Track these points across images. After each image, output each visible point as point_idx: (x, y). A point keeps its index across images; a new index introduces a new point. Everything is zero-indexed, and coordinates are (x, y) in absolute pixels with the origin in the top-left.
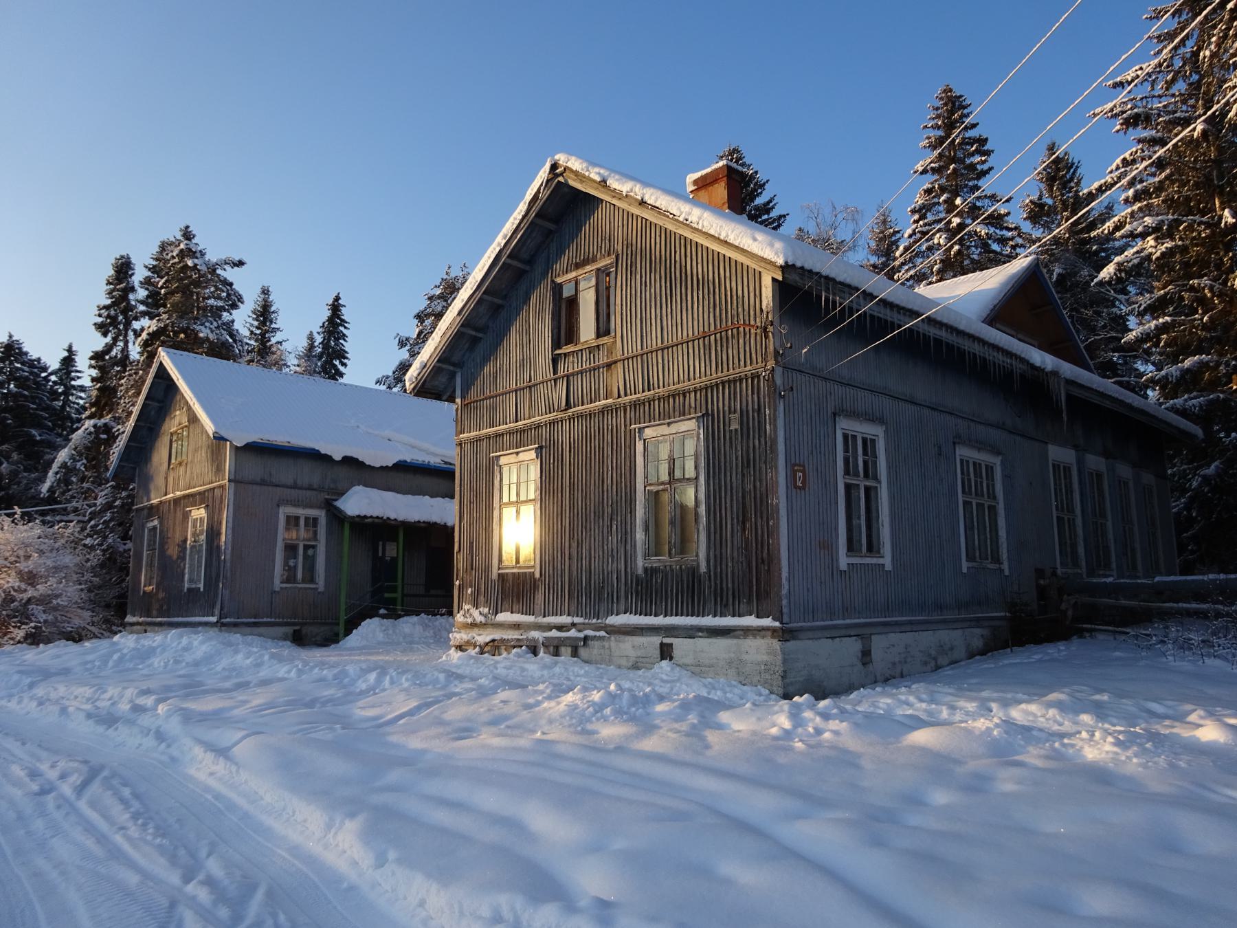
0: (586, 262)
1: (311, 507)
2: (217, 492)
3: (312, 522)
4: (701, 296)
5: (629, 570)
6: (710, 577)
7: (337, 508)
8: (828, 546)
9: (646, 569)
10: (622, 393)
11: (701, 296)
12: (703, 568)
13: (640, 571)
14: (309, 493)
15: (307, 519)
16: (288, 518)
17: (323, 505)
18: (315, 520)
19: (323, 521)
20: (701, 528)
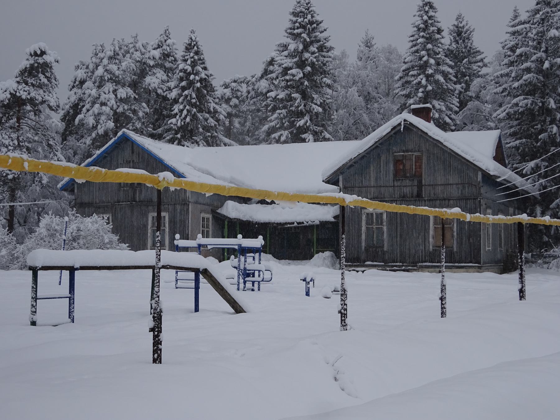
0: (407, 151)
1: (208, 213)
2: (178, 207)
3: (208, 219)
4: (456, 172)
5: (426, 249)
6: (457, 253)
7: (219, 214)
8: (485, 246)
9: (433, 250)
10: (424, 196)
11: (456, 172)
12: (455, 249)
13: (431, 250)
14: (207, 207)
15: (207, 219)
16: (202, 218)
17: (210, 212)
18: (208, 219)
19: (211, 219)
20: (455, 239)
